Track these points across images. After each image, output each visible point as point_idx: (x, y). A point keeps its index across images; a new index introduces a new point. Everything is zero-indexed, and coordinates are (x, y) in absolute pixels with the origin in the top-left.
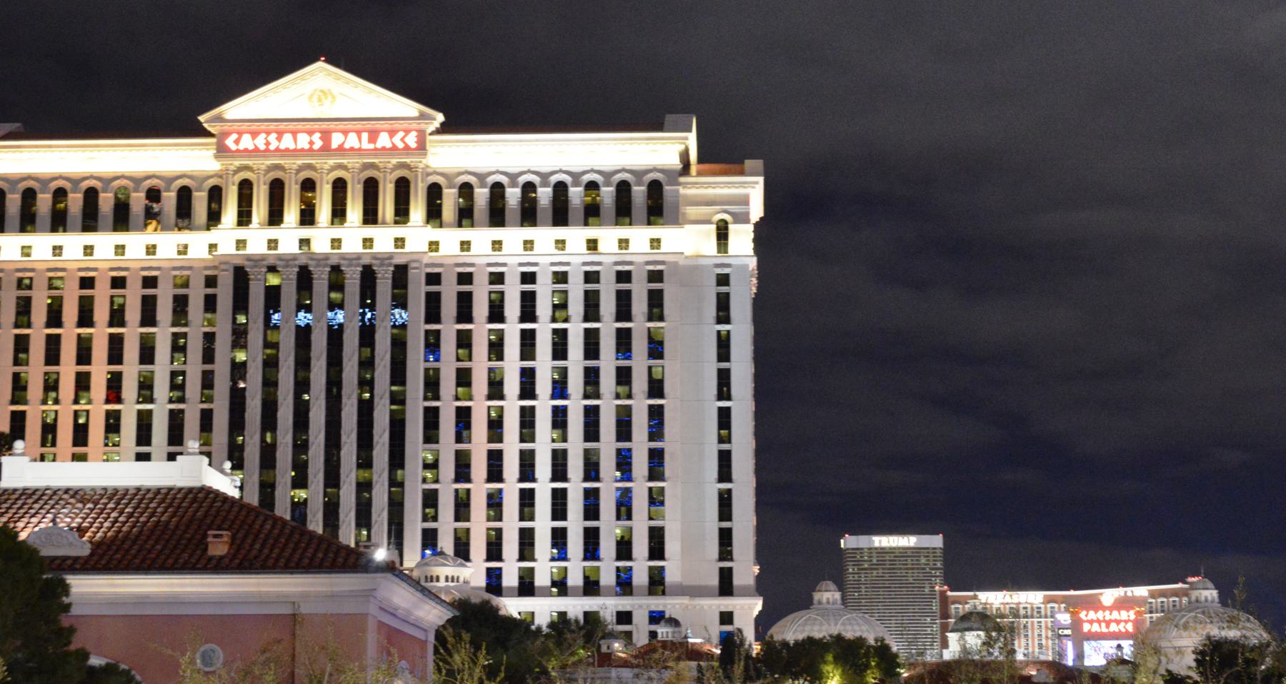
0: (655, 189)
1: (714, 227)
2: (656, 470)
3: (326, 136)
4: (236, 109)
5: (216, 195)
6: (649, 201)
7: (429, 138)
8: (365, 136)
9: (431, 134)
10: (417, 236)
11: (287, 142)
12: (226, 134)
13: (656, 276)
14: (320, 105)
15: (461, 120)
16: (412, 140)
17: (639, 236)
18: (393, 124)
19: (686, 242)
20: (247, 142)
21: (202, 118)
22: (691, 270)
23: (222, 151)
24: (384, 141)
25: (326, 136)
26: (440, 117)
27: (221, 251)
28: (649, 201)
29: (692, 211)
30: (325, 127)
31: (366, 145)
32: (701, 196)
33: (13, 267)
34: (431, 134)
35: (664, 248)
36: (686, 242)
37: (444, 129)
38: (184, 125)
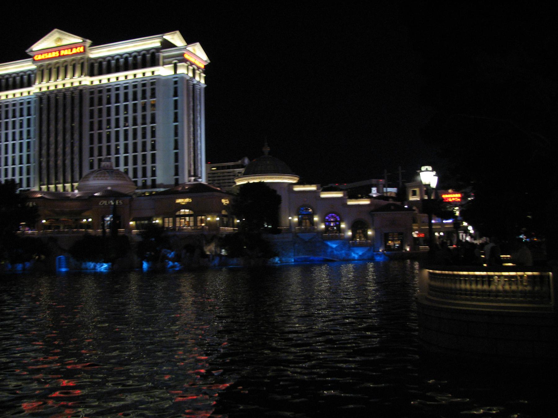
0: (153, 55)
1: (172, 65)
2: (153, 147)
3: (59, 53)
4: (36, 47)
5: (35, 74)
6: (149, 59)
7: (87, 49)
8: (70, 50)
9: (90, 47)
10: (87, 81)
11: (50, 55)
12: (34, 56)
13: (153, 84)
14: (53, 43)
15: (97, 42)
16: (81, 49)
17: (148, 71)
18: (76, 45)
19: (164, 71)
20: (39, 57)
21: (27, 51)
22: (165, 81)
23: (34, 61)
24: (75, 51)
25: (59, 53)
26: (89, 42)
27: (103, 82)
28: (149, 59)
29: (166, 60)
30: (58, 49)
31: (70, 53)
32: (171, 55)
33: (105, 85)
34: (90, 47)
35: (156, 74)
36: (164, 71)
37: (92, 45)
38: (22, 54)
